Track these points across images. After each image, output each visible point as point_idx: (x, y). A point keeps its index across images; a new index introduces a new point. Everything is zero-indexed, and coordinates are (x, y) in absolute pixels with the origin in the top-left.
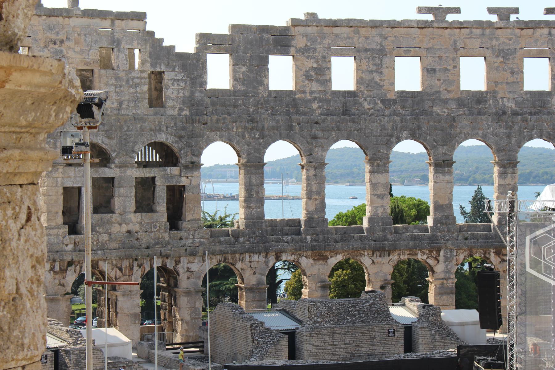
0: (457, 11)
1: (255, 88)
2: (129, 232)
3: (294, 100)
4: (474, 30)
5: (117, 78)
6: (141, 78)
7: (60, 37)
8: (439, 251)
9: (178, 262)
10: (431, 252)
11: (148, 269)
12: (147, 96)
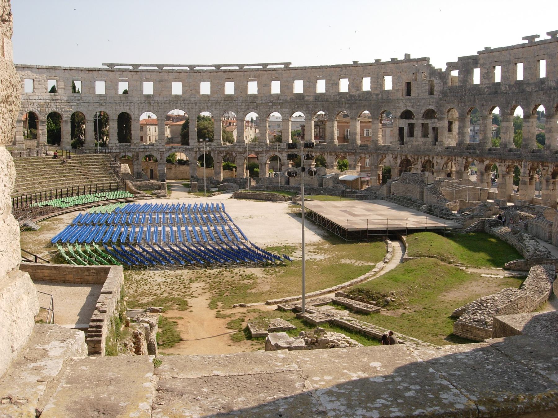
0: (538, 36)
2: (418, 145)
3: (479, 88)
4: (541, 45)
6: (425, 84)
7: (400, 71)
8: (522, 162)
9: (433, 158)
10: (519, 162)
11: (423, 161)
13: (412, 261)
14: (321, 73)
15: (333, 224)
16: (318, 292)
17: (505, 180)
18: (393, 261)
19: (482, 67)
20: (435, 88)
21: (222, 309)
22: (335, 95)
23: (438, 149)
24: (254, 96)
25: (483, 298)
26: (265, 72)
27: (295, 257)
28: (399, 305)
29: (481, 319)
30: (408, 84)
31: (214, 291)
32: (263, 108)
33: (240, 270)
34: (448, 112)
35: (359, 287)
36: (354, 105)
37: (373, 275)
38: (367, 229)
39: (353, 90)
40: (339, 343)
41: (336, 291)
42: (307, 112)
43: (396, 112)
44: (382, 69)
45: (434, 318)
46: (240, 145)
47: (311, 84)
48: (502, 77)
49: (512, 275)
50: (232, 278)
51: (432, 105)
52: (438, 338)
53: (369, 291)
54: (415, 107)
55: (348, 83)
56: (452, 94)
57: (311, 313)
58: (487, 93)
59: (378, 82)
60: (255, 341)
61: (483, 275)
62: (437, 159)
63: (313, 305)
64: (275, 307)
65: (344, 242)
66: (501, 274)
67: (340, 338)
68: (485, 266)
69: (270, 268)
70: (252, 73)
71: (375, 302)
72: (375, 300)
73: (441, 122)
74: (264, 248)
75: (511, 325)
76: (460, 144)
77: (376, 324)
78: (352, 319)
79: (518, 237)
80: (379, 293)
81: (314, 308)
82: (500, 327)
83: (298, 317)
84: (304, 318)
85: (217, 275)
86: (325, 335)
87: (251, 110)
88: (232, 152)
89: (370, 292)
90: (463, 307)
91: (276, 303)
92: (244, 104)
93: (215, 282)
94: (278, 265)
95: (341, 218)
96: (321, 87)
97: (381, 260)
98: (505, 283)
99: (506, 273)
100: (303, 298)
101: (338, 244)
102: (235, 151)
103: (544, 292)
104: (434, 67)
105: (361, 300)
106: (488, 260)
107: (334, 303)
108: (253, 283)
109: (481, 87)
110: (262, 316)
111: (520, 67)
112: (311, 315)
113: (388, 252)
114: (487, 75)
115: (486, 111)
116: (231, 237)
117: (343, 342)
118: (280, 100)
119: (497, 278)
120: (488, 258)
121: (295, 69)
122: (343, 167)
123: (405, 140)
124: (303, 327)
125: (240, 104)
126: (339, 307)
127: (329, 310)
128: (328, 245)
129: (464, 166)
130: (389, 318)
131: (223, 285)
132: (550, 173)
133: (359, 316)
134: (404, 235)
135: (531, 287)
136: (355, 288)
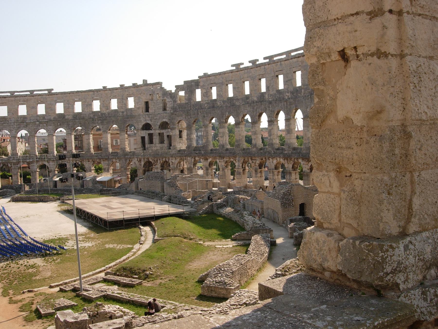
0: (243, 64)
1: (190, 101)
3: (201, 104)
5: (154, 103)
7: (140, 93)
8: (236, 157)
9: (169, 159)
11: (161, 162)
12: (162, 107)
13: (162, 241)
14: (78, 97)
15: (96, 217)
16: (91, 273)
17: (225, 172)
18: (146, 242)
19: (202, 88)
20: (167, 105)
21: (13, 296)
22: (89, 114)
23: (172, 152)
24: (24, 117)
25: (221, 264)
26: (32, 97)
27: (68, 246)
28: (157, 276)
29: (221, 280)
30: (147, 103)
31: (5, 281)
32: (31, 127)
33: (24, 261)
34: (178, 123)
35: (123, 266)
36: (105, 121)
37: (133, 255)
38: (124, 218)
39: (104, 109)
40: (115, 313)
41: (105, 270)
42: (68, 128)
43: (138, 125)
44: (125, 92)
45: (184, 284)
46: (14, 158)
47: (70, 105)
48: (218, 95)
49: (239, 244)
50: (18, 268)
51: (166, 119)
52: (190, 299)
53: (132, 268)
54: (153, 120)
55: (99, 104)
56: (181, 109)
57: (87, 291)
58: (207, 108)
59: (123, 102)
60: (45, 319)
61: (217, 246)
62: (172, 159)
63: (88, 285)
64: (57, 289)
65: (106, 231)
66: (230, 244)
67: (115, 309)
68: (217, 239)
69: (48, 258)
70: (21, 98)
71: (137, 276)
72: (137, 275)
73: (174, 131)
74: (41, 241)
75: (274, 288)
76: (189, 147)
77: (141, 294)
78: (122, 292)
79: (239, 215)
80: (139, 269)
81: (90, 286)
82: (264, 291)
83: (78, 296)
84: (83, 296)
85: (5, 267)
86: (104, 308)
87: (21, 128)
88: (7, 163)
89: (133, 269)
90: (206, 273)
91: (57, 286)
92: (16, 124)
93: (4, 274)
94: (55, 254)
95: (102, 212)
96: (78, 107)
97: (137, 243)
98: (234, 251)
99: (234, 243)
100: (80, 279)
101: (102, 233)
102: (10, 163)
103: (264, 254)
104: (166, 89)
105: (126, 276)
106: (219, 235)
107: (105, 281)
108: (36, 271)
109: (203, 103)
110: (48, 298)
111: (230, 87)
112: (88, 292)
113: (141, 235)
114: (206, 94)
115: (207, 121)
116: (13, 235)
117: (118, 312)
118: (46, 119)
119: (227, 247)
120: (219, 233)
121: (57, 94)
122: (99, 170)
123: (146, 147)
124: (83, 303)
125: (13, 124)
126: (109, 284)
127: (102, 286)
128: (93, 234)
129: (193, 163)
130: (150, 288)
131: (11, 276)
132: (257, 165)
133: (126, 289)
134: (153, 221)
135: (254, 252)
136: (120, 267)
